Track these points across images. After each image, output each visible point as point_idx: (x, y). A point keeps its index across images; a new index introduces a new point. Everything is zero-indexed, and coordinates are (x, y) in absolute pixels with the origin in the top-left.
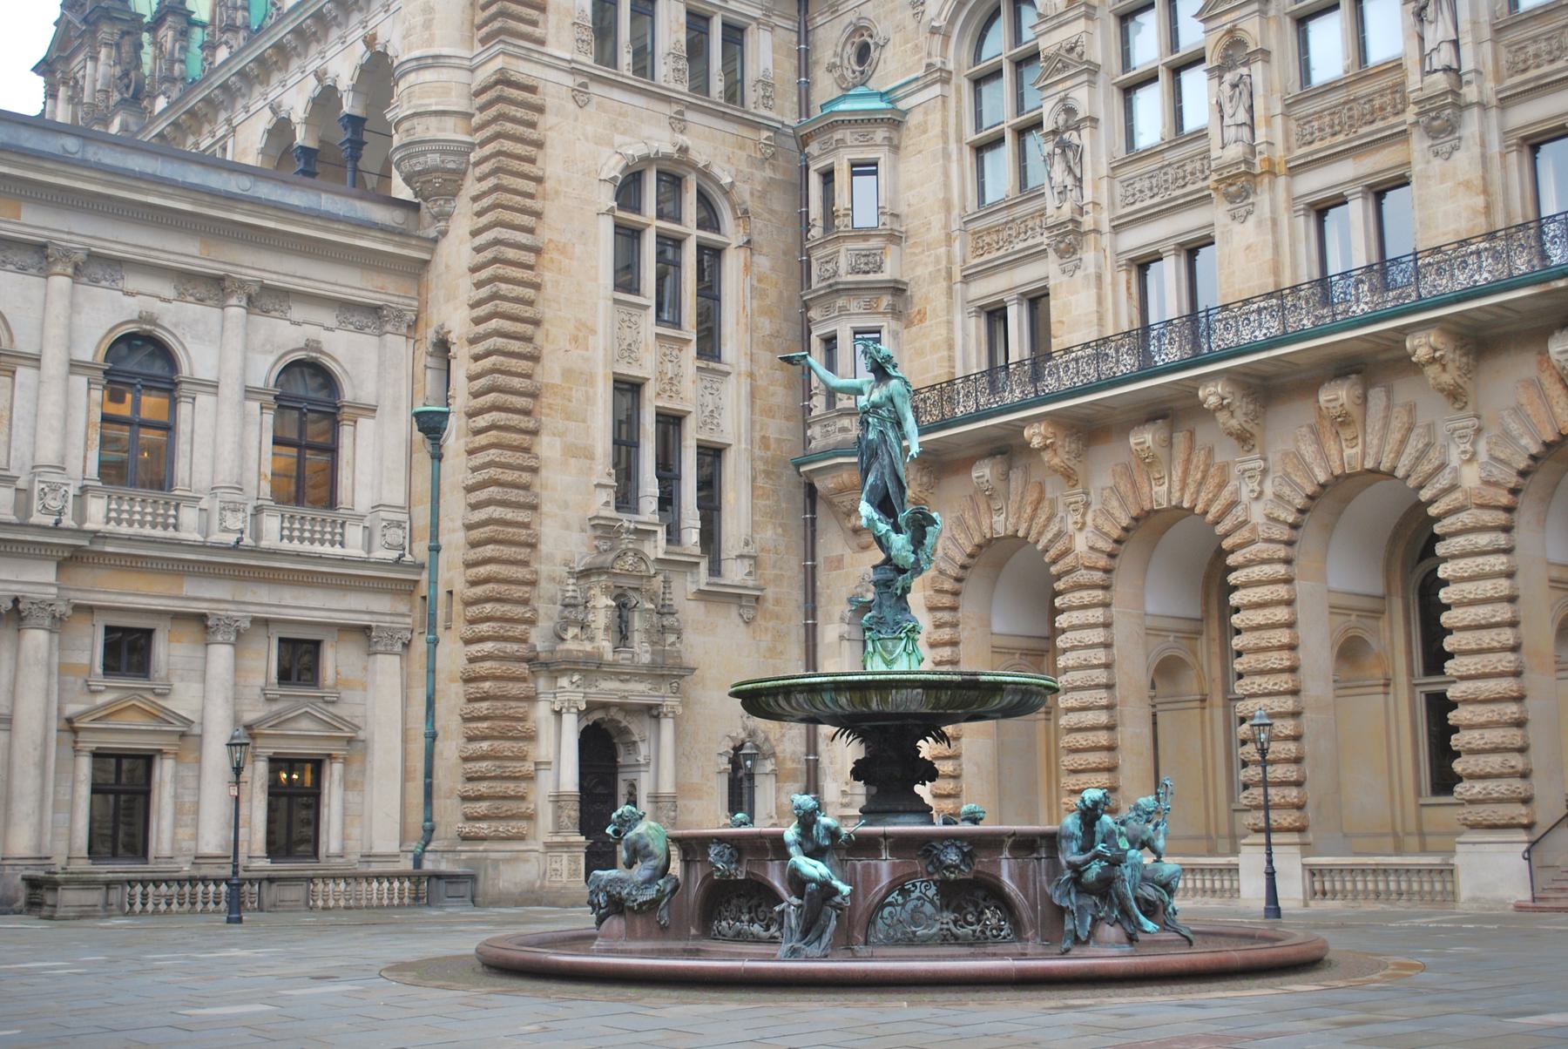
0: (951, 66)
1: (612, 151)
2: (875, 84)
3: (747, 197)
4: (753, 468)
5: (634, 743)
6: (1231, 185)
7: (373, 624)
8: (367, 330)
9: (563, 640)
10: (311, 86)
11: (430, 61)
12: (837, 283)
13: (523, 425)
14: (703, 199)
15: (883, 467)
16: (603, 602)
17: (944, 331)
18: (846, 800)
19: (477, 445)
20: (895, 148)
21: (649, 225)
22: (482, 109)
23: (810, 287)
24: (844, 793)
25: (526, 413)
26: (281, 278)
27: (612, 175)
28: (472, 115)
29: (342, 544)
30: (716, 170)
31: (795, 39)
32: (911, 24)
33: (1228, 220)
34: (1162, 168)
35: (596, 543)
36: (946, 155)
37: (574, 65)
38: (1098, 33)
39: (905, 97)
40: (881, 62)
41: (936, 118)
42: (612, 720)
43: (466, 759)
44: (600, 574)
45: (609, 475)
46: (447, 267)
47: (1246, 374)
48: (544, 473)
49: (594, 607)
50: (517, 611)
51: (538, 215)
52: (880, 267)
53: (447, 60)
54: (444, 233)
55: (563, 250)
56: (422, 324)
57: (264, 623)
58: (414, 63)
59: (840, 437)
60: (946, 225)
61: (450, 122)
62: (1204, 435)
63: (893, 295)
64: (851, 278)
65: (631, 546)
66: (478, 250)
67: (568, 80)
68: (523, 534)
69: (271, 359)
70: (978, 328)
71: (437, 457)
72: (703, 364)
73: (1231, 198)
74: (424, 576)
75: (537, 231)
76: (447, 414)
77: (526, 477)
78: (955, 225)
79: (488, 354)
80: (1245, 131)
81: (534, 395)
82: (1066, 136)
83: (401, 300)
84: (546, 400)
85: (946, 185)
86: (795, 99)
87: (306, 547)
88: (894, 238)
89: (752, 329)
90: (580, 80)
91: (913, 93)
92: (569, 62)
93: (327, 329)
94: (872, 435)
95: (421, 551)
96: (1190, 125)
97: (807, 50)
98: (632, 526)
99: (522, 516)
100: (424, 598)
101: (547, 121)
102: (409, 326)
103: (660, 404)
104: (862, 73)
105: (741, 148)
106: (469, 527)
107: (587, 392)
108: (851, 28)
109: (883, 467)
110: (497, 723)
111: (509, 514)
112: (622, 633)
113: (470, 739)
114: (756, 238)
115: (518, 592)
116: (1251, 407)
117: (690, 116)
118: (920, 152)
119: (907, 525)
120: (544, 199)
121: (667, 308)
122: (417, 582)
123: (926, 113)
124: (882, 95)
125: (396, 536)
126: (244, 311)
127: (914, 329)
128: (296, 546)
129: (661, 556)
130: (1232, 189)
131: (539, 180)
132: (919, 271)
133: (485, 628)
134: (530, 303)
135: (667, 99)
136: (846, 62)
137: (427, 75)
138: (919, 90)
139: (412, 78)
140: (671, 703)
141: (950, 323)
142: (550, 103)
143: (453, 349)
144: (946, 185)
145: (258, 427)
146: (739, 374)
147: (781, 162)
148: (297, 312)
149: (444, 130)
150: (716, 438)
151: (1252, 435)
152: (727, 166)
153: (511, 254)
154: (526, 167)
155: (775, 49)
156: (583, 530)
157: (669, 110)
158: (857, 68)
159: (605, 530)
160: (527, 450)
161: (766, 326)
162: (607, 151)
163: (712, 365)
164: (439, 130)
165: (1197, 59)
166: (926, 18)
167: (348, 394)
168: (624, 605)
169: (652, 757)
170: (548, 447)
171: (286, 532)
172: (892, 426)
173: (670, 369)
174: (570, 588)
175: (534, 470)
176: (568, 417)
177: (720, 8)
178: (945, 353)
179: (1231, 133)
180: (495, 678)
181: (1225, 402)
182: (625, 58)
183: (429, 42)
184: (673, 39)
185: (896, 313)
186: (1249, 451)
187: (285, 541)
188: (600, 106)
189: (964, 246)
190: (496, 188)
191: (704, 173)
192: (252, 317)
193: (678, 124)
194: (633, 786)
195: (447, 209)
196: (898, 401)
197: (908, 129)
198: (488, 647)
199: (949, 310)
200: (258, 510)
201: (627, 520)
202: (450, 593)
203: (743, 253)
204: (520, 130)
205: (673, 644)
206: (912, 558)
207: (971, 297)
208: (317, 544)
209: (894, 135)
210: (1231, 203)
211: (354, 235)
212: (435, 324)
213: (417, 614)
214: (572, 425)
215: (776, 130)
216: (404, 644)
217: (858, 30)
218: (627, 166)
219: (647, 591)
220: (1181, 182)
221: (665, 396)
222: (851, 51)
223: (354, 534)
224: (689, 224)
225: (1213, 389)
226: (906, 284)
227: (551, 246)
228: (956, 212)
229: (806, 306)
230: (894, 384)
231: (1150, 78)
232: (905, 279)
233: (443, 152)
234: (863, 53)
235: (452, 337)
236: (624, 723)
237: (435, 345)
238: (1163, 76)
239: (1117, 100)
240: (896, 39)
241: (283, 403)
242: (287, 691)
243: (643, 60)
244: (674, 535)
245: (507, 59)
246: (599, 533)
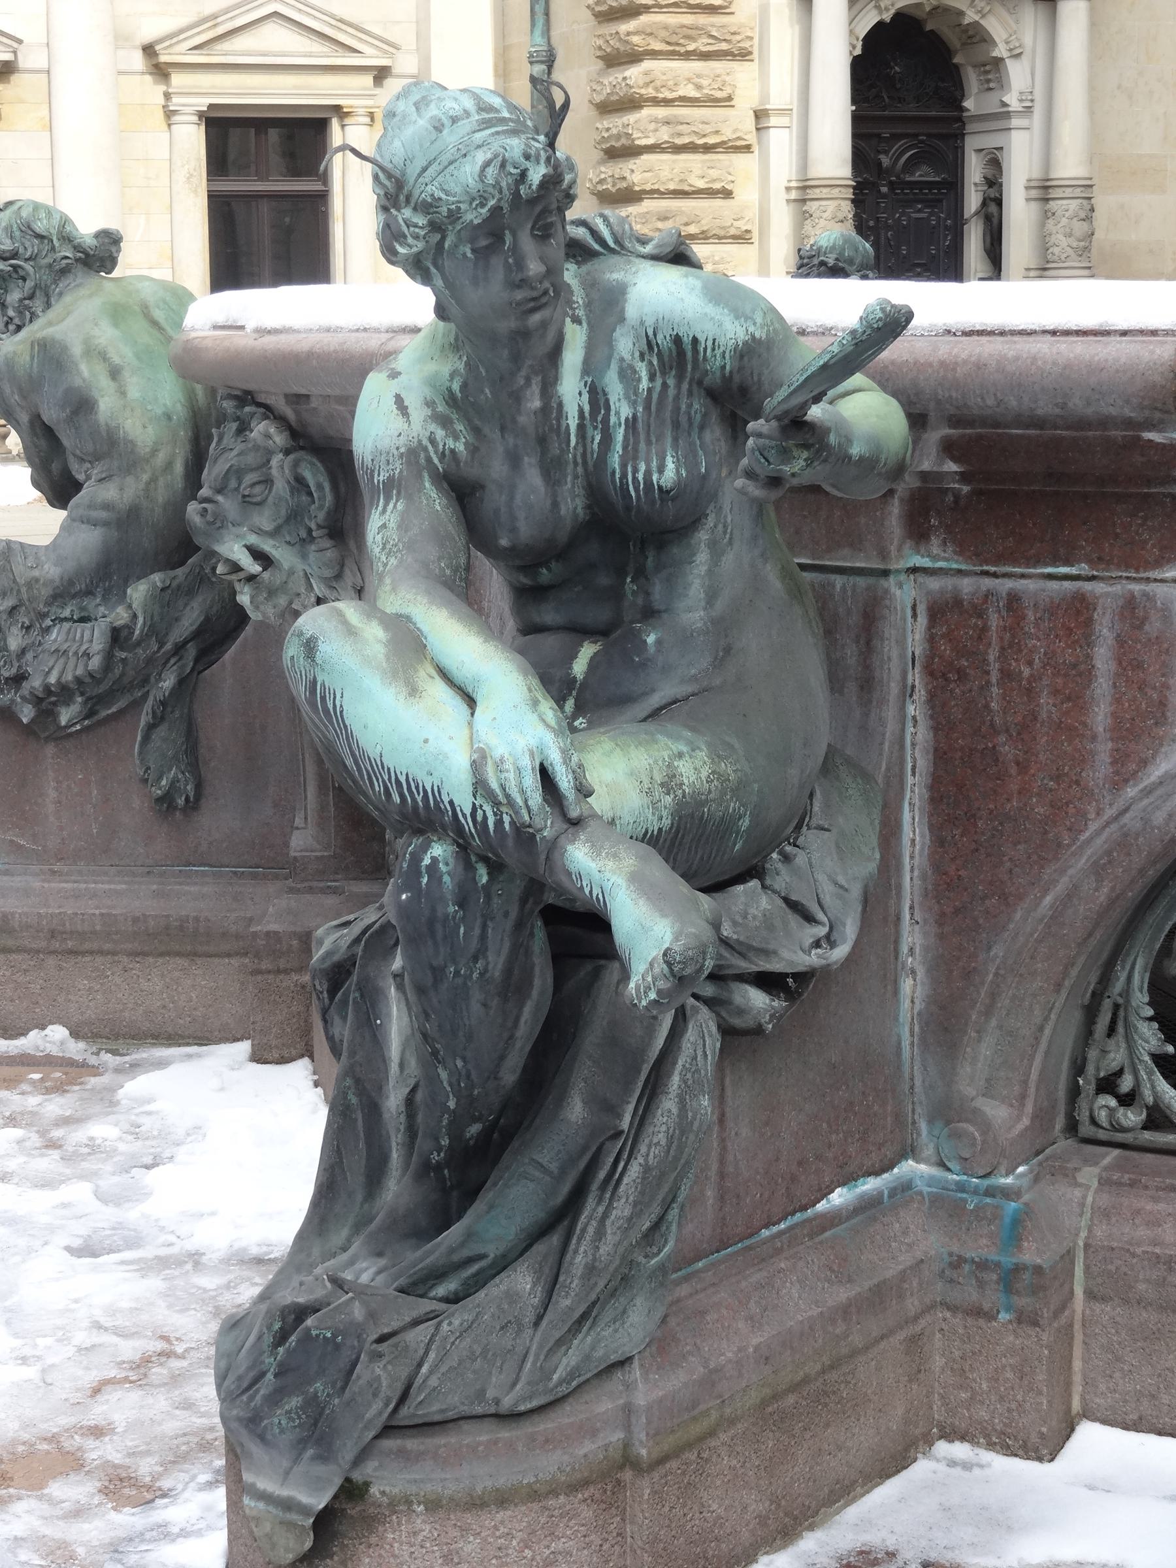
5: (999, 61)
169: (1039, 95)
194: (995, 164)
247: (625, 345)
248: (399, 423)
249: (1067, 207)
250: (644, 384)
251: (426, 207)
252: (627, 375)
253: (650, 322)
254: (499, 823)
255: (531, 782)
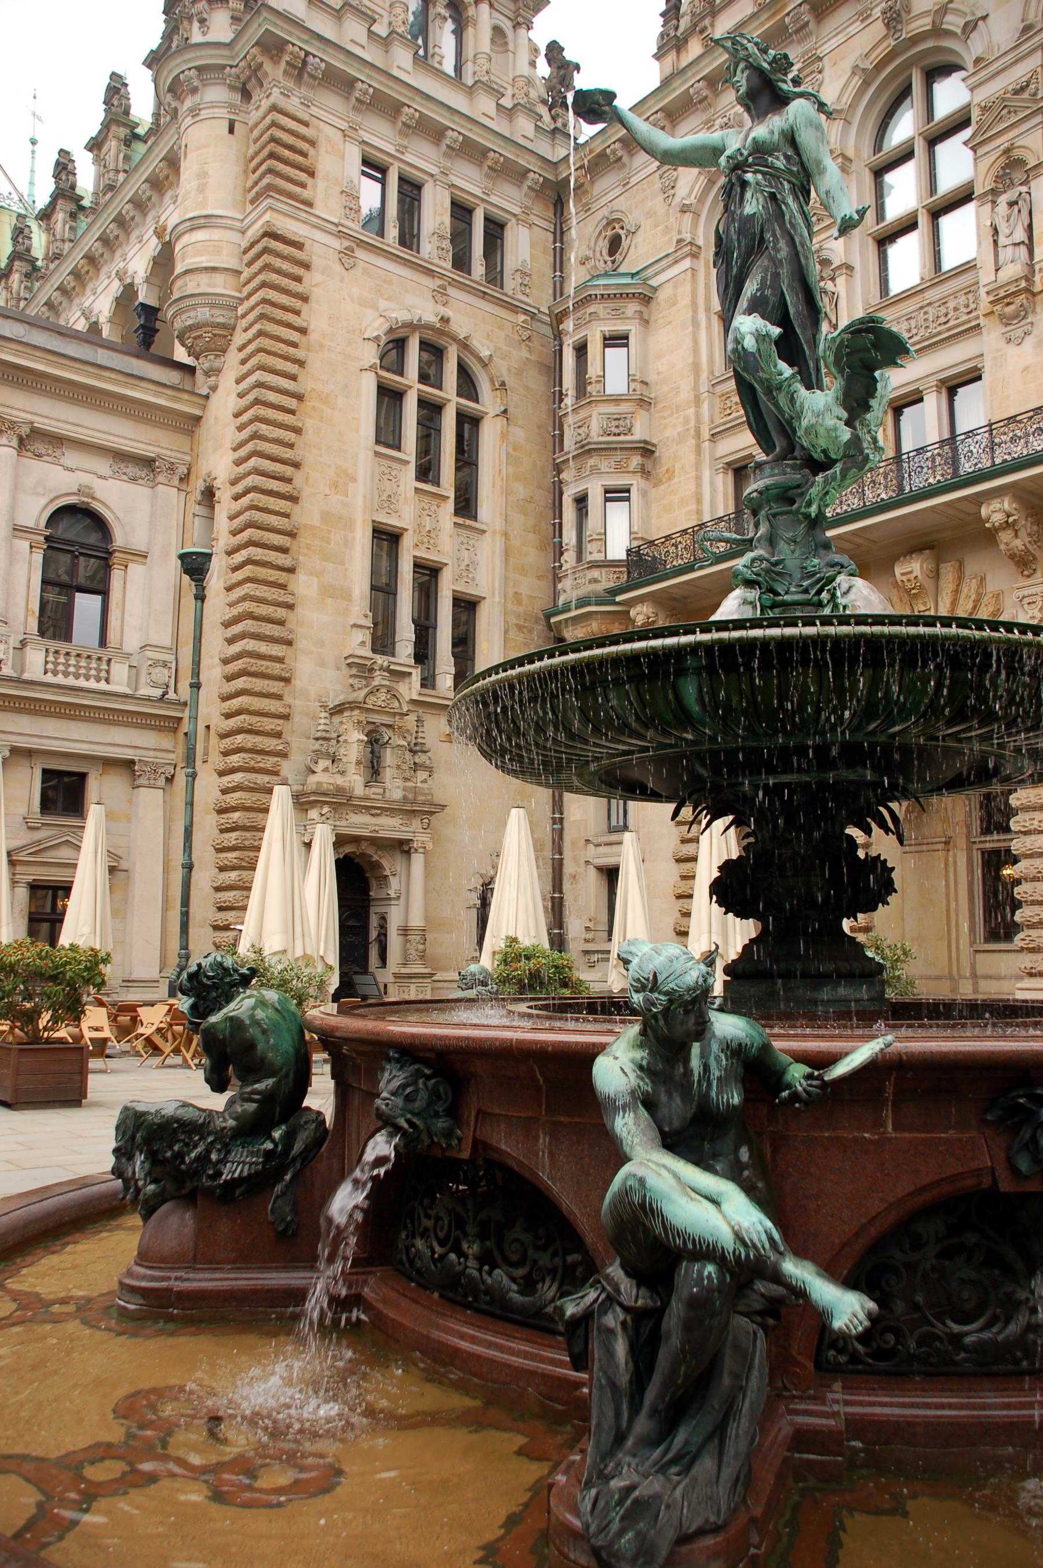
0: (700, 242)
1: (377, 314)
2: (621, 270)
3: (504, 372)
4: (506, 622)
6: (1008, 304)
7: (136, 758)
8: (140, 481)
9: (314, 772)
10: (116, 288)
11: (202, 221)
12: (589, 443)
13: (280, 562)
14: (464, 373)
15: (776, 263)
16: (356, 736)
17: (692, 487)
18: (590, 936)
19: (234, 581)
20: (646, 322)
21: (410, 387)
22: (249, 265)
23: (562, 450)
24: (587, 929)
25: (285, 551)
26: (54, 423)
27: (375, 334)
28: (241, 273)
29: (107, 681)
30: (475, 343)
31: (551, 238)
32: (660, 207)
33: (1002, 344)
34: (921, 308)
35: (351, 681)
36: (695, 323)
37: (340, 228)
38: (854, 185)
39: (656, 274)
40: (632, 250)
41: (687, 288)
42: (363, 855)
43: (218, 889)
44: (352, 709)
45: (366, 616)
46: (216, 418)
47: (1031, 493)
48: (299, 610)
49: (345, 741)
50: (270, 743)
51: (301, 363)
52: (630, 430)
53: (219, 220)
54: (214, 389)
55: (325, 399)
56: (192, 477)
57: (29, 754)
58: (188, 224)
59: (590, 588)
60: (696, 387)
61: (219, 278)
62: (974, 565)
63: (642, 456)
64: (601, 439)
65: (384, 682)
66: (241, 396)
67: (336, 244)
68: (276, 668)
69: (43, 501)
70: (725, 483)
71: (200, 597)
72: (460, 521)
73: (1006, 320)
74: (186, 715)
75: (299, 379)
76: (211, 555)
77: (281, 613)
78: (704, 387)
79: (247, 491)
80: (1023, 251)
81: (292, 535)
82: (822, 284)
83: (173, 454)
84: (303, 539)
85: (696, 351)
86: (551, 291)
87: (71, 681)
88: (644, 403)
89: (508, 492)
90: (346, 243)
91: (663, 270)
92: (337, 225)
93: (100, 477)
94: (752, 206)
95: (184, 692)
96: (949, 262)
97: (562, 249)
98: (386, 664)
99: (276, 650)
100: (186, 734)
101: (312, 279)
102: (181, 479)
103: (418, 554)
104: (613, 262)
105: (501, 328)
106: (226, 662)
107: (345, 536)
108: (605, 222)
109: (776, 263)
110: (246, 853)
111: (263, 648)
112: (374, 769)
113: (222, 869)
114: (511, 410)
115: (269, 724)
116: (1035, 528)
117: (451, 291)
118: (670, 323)
119: (837, 362)
120: (308, 350)
121: (427, 471)
122: (180, 719)
123: (675, 287)
124: (633, 275)
125: (162, 675)
126: (15, 452)
127: (662, 487)
128: (60, 679)
129: (415, 697)
130: (1010, 309)
131: (303, 331)
132: (668, 433)
133: (235, 760)
134: (291, 446)
135: (430, 273)
136: (598, 255)
137: (200, 235)
138: (669, 266)
139: (186, 239)
140: (421, 838)
141: (698, 479)
142: (316, 261)
143: (218, 494)
144: (696, 351)
145: (26, 565)
146: (494, 533)
147: (535, 344)
148: (71, 458)
149: (214, 286)
150: (471, 590)
151: (1035, 558)
152: (486, 342)
153: (272, 397)
154: (290, 317)
155: (532, 245)
156: (338, 669)
157: (434, 283)
158: (608, 258)
159: (363, 670)
160: (283, 587)
161: (521, 491)
162: (371, 314)
163: (468, 522)
164: (209, 285)
165: (962, 198)
166: (677, 200)
167: (119, 539)
168: (377, 741)
170: (304, 585)
171: (50, 666)
172: (793, 191)
173: (428, 523)
174: (322, 721)
175: (290, 607)
176: (326, 558)
177: (483, 200)
178: (694, 507)
179: (1006, 254)
180: (245, 809)
181: (1011, 519)
182: (392, 232)
183: (203, 205)
184: (438, 220)
185: (645, 473)
186: (1028, 576)
187: (49, 674)
188: (365, 271)
189: (711, 407)
190: (261, 334)
191: (464, 345)
192: (24, 460)
193: (440, 295)
194: (383, 919)
195: (217, 364)
196: (806, 138)
197: (658, 304)
198: (238, 777)
199: (698, 466)
200: (23, 643)
201: (381, 660)
202: (208, 727)
203: (501, 422)
204: (285, 282)
205: (425, 781)
206: (846, 434)
207: (719, 454)
208: (82, 679)
209: (644, 309)
210: (1007, 325)
211: (126, 385)
212: (204, 471)
213: (181, 750)
214: (330, 566)
215: (533, 316)
216: (167, 779)
217: (610, 223)
218: (391, 330)
219: (400, 728)
220: (943, 320)
221: (423, 547)
222: (604, 245)
223: (120, 673)
224: (449, 390)
225: (998, 506)
226: (654, 445)
227: (314, 394)
228: (704, 376)
229: (558, 469)
230: (798, 108)
231: (908, 225)
232: (654, 441)
233: (213, 306)
234: (615, 245)
235: (217, 484)
236: (376, 858)
237: (203, 493)
238: (923, 220)
239: (872, 248)
240: (646, 224)
241: (54, 546)
242: (49, 820)
243: (409, 238)
244: (428, 681)
245: (275, 215)
246: (354, 671)
247: (715, 1047)
248: (624, 1079)
249: (415, 938)
250: (724, 1062)
251: (666, 993)
252: (718, 1059)
253: (729, 1037)
254: (747, 1255)
255: (764, 1237)
